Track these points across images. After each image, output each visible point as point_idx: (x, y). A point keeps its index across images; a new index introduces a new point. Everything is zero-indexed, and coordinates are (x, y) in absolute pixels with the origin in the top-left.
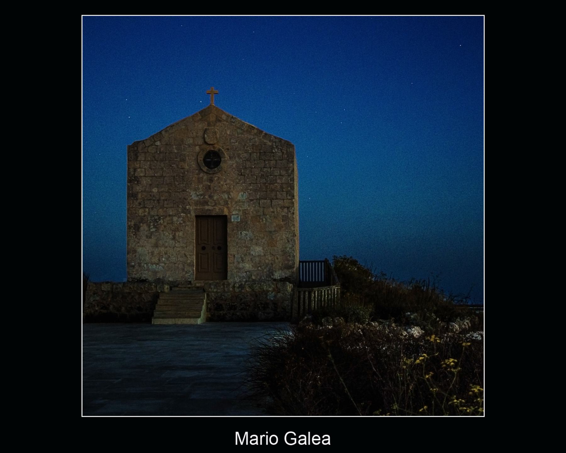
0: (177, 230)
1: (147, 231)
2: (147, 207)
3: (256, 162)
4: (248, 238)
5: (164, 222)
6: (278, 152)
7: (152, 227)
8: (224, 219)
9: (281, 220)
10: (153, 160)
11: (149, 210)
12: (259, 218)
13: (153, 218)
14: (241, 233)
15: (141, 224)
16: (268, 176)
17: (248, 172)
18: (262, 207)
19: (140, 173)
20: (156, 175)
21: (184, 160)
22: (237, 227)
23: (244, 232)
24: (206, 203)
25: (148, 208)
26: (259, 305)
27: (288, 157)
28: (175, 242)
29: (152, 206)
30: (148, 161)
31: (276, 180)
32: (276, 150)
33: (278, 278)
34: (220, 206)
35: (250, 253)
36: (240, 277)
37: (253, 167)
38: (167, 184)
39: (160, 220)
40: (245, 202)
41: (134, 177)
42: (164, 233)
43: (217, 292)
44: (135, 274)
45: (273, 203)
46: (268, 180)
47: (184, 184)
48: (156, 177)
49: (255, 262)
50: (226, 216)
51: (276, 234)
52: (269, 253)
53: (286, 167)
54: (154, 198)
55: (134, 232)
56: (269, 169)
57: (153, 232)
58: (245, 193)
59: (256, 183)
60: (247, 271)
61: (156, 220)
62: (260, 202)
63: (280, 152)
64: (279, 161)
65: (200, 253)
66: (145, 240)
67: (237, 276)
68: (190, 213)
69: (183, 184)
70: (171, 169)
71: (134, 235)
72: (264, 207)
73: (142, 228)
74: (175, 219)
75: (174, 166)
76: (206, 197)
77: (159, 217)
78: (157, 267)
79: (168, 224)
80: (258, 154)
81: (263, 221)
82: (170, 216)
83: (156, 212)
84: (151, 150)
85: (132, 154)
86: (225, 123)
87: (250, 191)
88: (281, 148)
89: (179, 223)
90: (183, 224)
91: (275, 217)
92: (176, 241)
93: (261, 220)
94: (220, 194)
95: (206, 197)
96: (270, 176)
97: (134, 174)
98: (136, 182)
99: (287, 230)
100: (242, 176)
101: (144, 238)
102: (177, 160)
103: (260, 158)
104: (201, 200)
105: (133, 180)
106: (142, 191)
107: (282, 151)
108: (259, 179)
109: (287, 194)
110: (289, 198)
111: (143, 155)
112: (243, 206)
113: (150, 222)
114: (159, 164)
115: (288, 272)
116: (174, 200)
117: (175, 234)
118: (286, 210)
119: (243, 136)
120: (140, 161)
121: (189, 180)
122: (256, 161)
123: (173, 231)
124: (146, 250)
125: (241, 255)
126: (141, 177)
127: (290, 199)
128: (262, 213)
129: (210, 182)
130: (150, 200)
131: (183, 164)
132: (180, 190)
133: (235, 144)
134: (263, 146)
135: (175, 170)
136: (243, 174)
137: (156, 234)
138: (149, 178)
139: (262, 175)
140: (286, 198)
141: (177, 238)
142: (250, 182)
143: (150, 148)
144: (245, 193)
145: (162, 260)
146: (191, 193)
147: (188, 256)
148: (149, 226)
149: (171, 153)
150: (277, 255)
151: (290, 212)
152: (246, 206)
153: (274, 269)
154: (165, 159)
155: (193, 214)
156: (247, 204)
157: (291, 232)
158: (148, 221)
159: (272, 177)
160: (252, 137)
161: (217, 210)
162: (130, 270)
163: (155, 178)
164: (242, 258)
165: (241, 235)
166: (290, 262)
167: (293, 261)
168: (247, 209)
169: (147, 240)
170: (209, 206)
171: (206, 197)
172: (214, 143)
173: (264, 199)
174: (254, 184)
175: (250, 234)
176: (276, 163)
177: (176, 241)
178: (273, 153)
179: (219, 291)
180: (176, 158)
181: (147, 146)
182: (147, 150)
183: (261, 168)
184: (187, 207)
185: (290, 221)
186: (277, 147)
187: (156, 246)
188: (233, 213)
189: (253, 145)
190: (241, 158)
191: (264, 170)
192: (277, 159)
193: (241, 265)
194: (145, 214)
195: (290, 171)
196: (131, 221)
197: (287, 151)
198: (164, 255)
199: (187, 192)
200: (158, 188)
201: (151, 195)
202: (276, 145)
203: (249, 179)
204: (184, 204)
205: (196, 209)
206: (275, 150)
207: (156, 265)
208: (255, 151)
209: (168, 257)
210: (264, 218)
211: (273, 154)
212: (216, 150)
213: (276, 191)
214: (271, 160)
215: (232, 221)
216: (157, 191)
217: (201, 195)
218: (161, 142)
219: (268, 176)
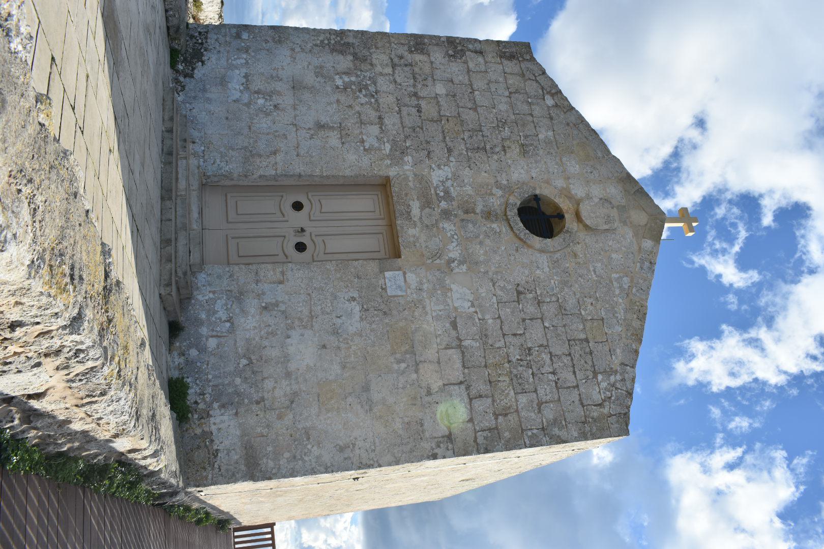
0: (344, 135)
1: (333, 67)
2: (397, 72)
3: (561, 330)
4: (339, 321)
5: (362, 104)
6: (600, 392)
7: (346, 79)
9: (406, 420)
10: (508, 89)
11: (390, 74)
12: (403, 349)
13: (369, 82)
14: (353, 299)
15: (350, 58)
16: (531, 368)
17: (531, 309)
18: (439, 359)
19: (475, 62)
20: (476, 93)
21: (524, 150)
23: (358, 308)
24: (427, 203)
25: (393, 71)
27: (595, 420)
28: (309, 129)
29: (399, 81)
30: (505, 78)
31: (524, 392)
32: (604, 385)
33: (215, 424)
34: (423, 238)
35: (290, 327)
36: (213, 301)
37: (547, 324)
38: (458, 114)
39: (365, 96)
40: (447, 307)
41: (462, 50)
42: (332, 103)
45: (456, 387)
46: (520, 368)
47: (467, 151)
48: (471, 93)
49: (266, 347)
50: (398, 255)
51: (362, 406)
52: (295, 387)
53: (566, 421)
54: (419, 86)
55: (330, 43)
56: (551, 370)
57: (334, 81)
58: (473, 305)
59: (504, 335)
60: (232, 324)
61: (366, 87)
62: (452, 348)
63: (603, 397)
64: (578, 396)
65: (282, 196)
66: (310, 64)
67: (214, 292)
69: (467, 149)
70: (498, 126)
72: (439, 363)
73: (341, 57)
74: (375, 130)
76: (443, 204)
77: (373, 96)
78: (237, 87)
79: (358, 112)
80: (583, 336)
81: (399, 362)
82: (380, 118)
84: (531, 87)
85: (514, 50)
86: (636, 247)
87: (479, 319)
88: (613, 398)
89: (363, 138)
90: (362, 148)
91: (415, 398)
92: (312, 132)
93: (398, 356)
94: (456, 237)
95: (443, 204)
96: (533, 374)
97: (469, 50)
98: (451, 52)
99: (377, 440)
100: (515, 294)
101: (316, 62)
102: (522, 138)
103: (574, 340)
105: (456, 47)
106: (432, 63)
107: (604, 401)
108: (517, 341)
109: (490, 429)
111: (516, 69)
113: (357, 76)
114: (503, 100)
115: (236, 457)
116: (422, 129)
117: (332, 128)
118: (440, 435)
119: (617, 292)
120: (501, 63)
121: (478, 164)
122: (563, 330)
123: (340, 124)
124: (285, 64)
125: (282, 302)
126: (466, 62)
127: (476, 438)
128: (422, 359)
129: (482, 211)
130: (414, 78)
132: (450, 144)
133: (593, 273)
134: (607, 348)
135: (497, 132)
136: (522, 297)
137: (329, 89)
138: (467, 77)
139: (530, 349)
140: (477, 428)
141: (322, 133)
142: (503, 317)
143: (535, 84)
144: (473, 305)
145: (259, 98)
146: (446, 167)
147: (272, 159)
148: (344, 73)
149: (535, 127)
150: (291, 416)
151: (439, 446)
152: (433, 307)
153: (242, 410)
154: (519, 114)
155: (392, 172)
156: (440, 313)
157: (372, 455)
158: (361, 71)
159: (531, 380)
160: (621, 315)
161: (412, 231)
163: (471, 91)
164: (277, 304)
166: (271, 464)
167: (274, 471)
168: (426, 313)
171: (443, 201)
172: (584, 219)
173: (463, 362)
174: (501, 328)
175: (353, 325)
176: (569, 387)
177: (312, 132)
178: (595, 376)
180: (526, 137)
181: (538, 79)
182: (530, 79)
183: (548, 346)
184: (408, 159)
185: (409, 447)
186: (613, 385)
187: (297, 86)
188: (409, 275)
189: (603, 319)
190: (562, 290)
191: (544, 356)
192: (582, 390)
193: (252, 305)
194: (379, 66)
196: (355, 37)
197: (611, 415)
198: (271, 103)
199: (448, 157)
200: (447, 95)
201: (425, 80)
202: (616, 381)
203: (513, 312)
204: (417, 150)
205: (406, 178)
206: (603, 380)
208: (588, 324)
209: (268, 111)
210: (408, 366)
211: (593, 378)
212: (567, 225)
213: (493, 396)
214: (574, 373)
216: (438, 92)
217: (447, 192)
219: (531, 368)
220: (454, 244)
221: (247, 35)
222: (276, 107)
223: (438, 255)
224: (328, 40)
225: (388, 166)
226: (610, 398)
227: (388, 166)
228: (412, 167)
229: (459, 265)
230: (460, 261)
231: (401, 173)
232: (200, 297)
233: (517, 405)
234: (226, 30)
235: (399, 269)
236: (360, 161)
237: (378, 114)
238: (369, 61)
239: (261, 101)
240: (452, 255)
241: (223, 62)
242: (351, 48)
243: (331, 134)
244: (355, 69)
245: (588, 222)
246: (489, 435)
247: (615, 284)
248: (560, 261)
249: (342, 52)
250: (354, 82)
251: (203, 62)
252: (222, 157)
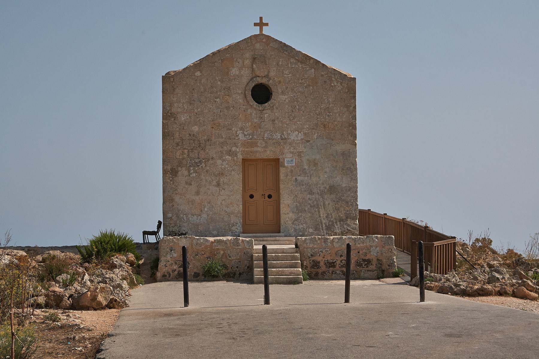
5: (206, 166)
6: (338, 86)
8: (276, 163)
13: (193, 162)
15: (180, 169)
22: (292, 171)
26: (362, 262)
28: (220, 190)
32: (336, 84)
37: (310, 102)
41: (170, 113)
43: (313, 248)
44: (173, 227)
50: (279, 159)
57: (194, 177)
68: (236, 155)
71: (171, 181)
73: (179, 173)
75: (217, 100)
78: (199, 219)
83: (197, 155)
88: (341, 81)
97: (170, 110)
102: (221, 93)
104: (249, 140)
107: (342, 85)
110: (350, 138)
112: (297, 148)
113: (190, 166)
131: (228, 98)
148: (189, 172)
155: (240, 157)
162: (167, 222)
165: (297, 181)
168: (303, 151)
169: (186, 187)
170: (258, 148)
179: (315, 246)
184: (234, 149)
195: (351, 108)
201: (190, 135)
205: (244, 151)
206: (334, 83)
207: (197, 216)
215: (286, 165)
217: (250, 135)
218: (201, 72)
220: (274, 135)
221: (169, 214)
222: (209, 203)
223: (279, 143)
224: (170, 178)
225: (237, 158)
226: (341, 82)
227: (237, 158)
228: (237, 148)
229: (283, 135)
230: (282, 134)
231: (240, 153)
232: (293, 234)
233: (340, 122)
234: (167, 223)
235: (284, 159)
236: (235, 170)
237: (211, 160)
238: (181, 160)
239: (206, 209)
240: (279, 137)
241: (185, 225)
242: (174, 167)
243: (222, 180)
244: (186, 167)
245: (266, 73)
246: (350, 135)
247: (293, 66)
248: (282, 90)
249: (177, 172)
250: (193, 168)
251: (186, 233)
252: (234, 226)
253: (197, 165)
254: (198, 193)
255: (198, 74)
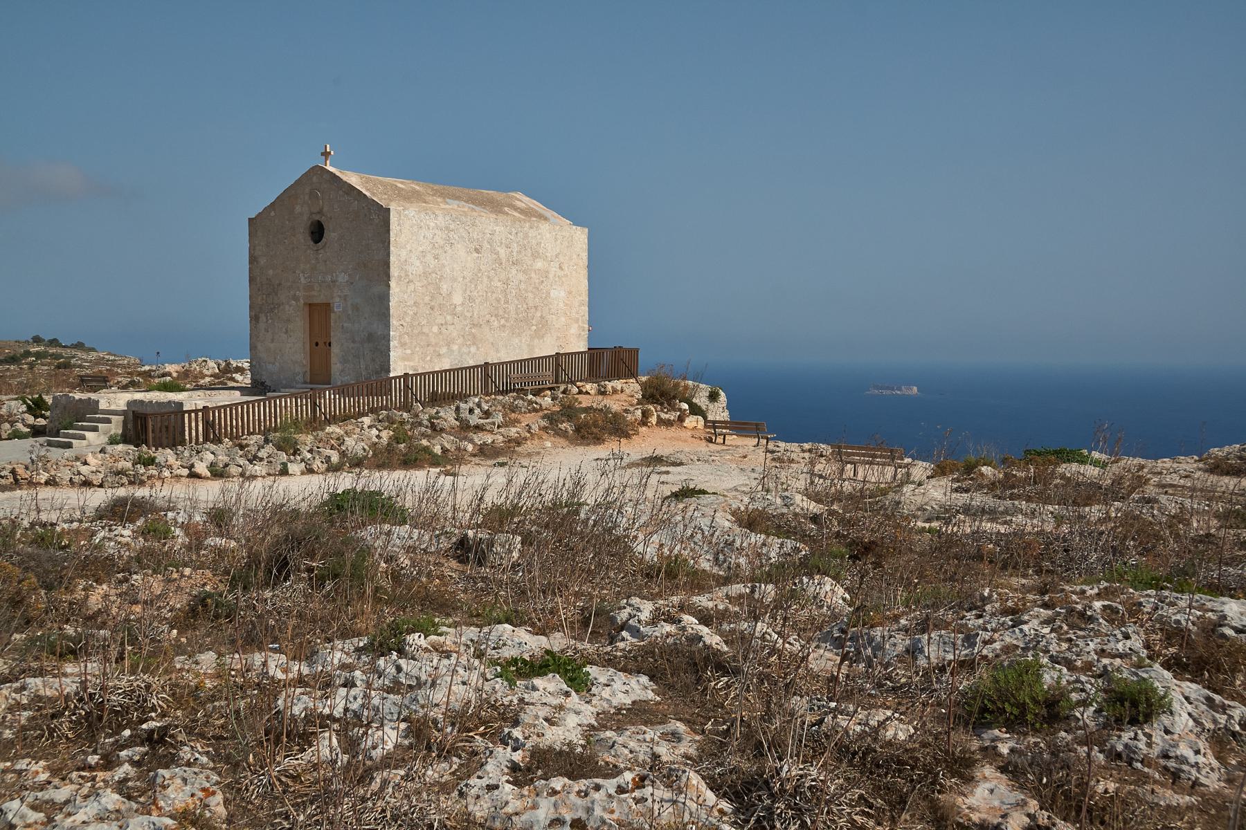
68: (299, 301)
73: (261, 319)
101: (263, 331)
110: (385, 279)
155: (302, 301)
253: (272, 310)
254: (272, 341)
255: (273, 214)
